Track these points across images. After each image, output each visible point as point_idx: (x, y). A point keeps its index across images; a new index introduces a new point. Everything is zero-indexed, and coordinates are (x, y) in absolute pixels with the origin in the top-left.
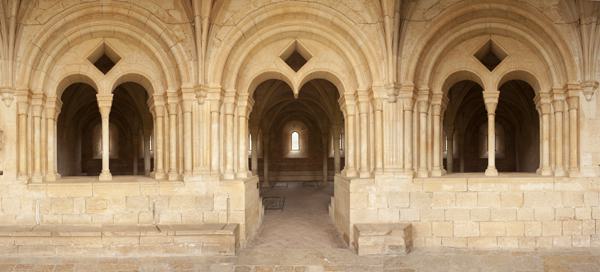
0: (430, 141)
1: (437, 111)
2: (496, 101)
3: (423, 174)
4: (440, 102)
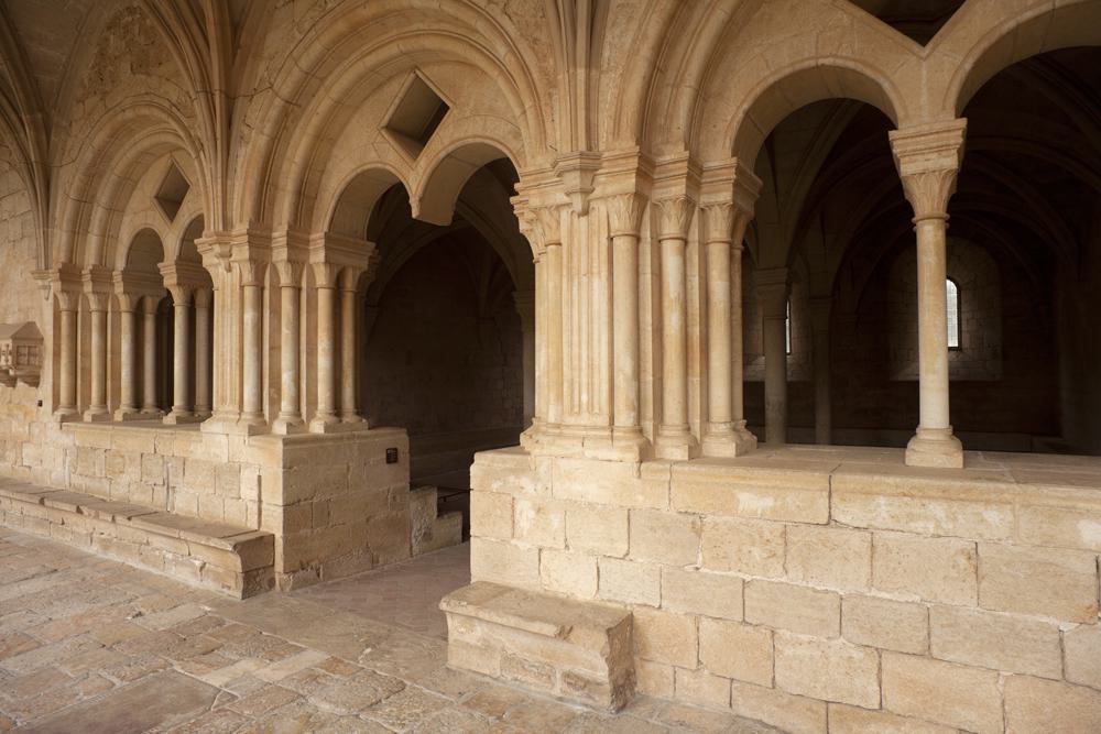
0: (696, 331)
1: (719, 227)
2: (951, 162)
3: (673, 449)
4: (726, 196)
